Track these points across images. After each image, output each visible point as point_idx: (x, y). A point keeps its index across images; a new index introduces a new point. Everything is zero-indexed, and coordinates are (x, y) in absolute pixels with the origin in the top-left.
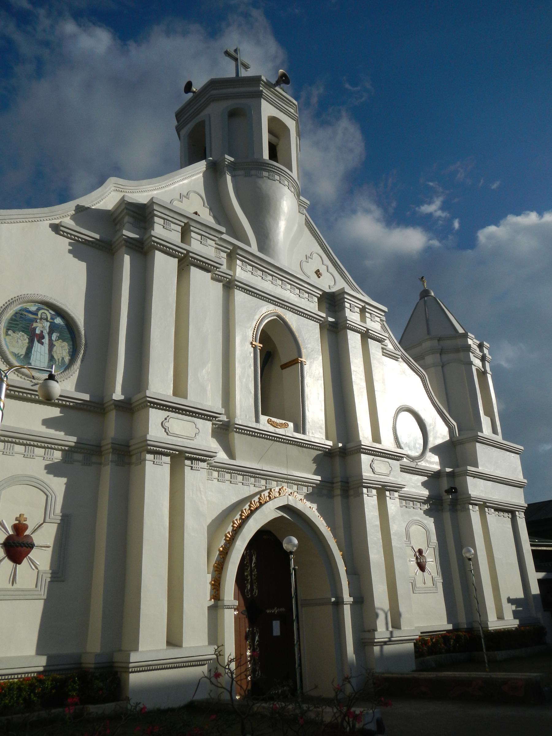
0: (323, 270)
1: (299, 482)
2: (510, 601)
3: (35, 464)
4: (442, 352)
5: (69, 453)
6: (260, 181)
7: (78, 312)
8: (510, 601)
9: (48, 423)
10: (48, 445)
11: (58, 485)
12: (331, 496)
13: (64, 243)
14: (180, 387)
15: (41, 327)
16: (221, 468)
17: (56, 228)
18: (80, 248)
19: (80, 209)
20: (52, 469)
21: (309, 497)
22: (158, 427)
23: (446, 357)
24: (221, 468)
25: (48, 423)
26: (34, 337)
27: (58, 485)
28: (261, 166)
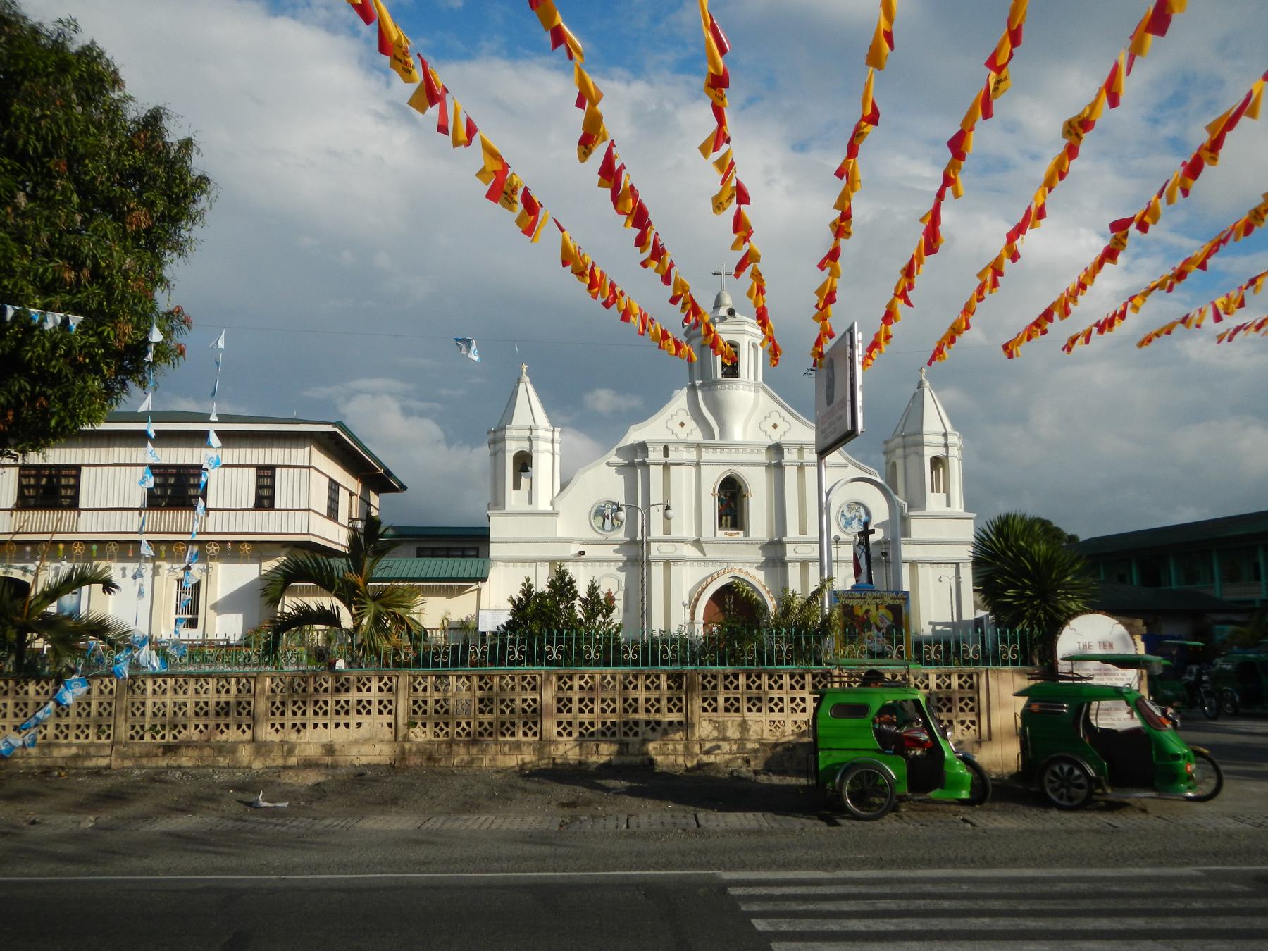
0: (779, 422)
1: (750, 562)
2: (930, 623)
3: (612, 569)
4: (904, 447)
5: (625, 563)
6: (717, 393)
7: (621, 500)
8: (930, 623)
9: (616, 551)
10: (616, 561)
11: (622, 575)
12: (775, 566)
13: (613, 469)
14: (667, 531)
15: (608, 512)
16: (698, 561)
17: (608, 464)
18: (620, 469)
19: (618, 450)
20: (619, 569)
21: (758, 568)
22: (655, 551)
23: (909, 450)
24: (698, 561)
25: (616, 551)
26: (605, 517)
27: (622, 575)
28: (716, 383)
